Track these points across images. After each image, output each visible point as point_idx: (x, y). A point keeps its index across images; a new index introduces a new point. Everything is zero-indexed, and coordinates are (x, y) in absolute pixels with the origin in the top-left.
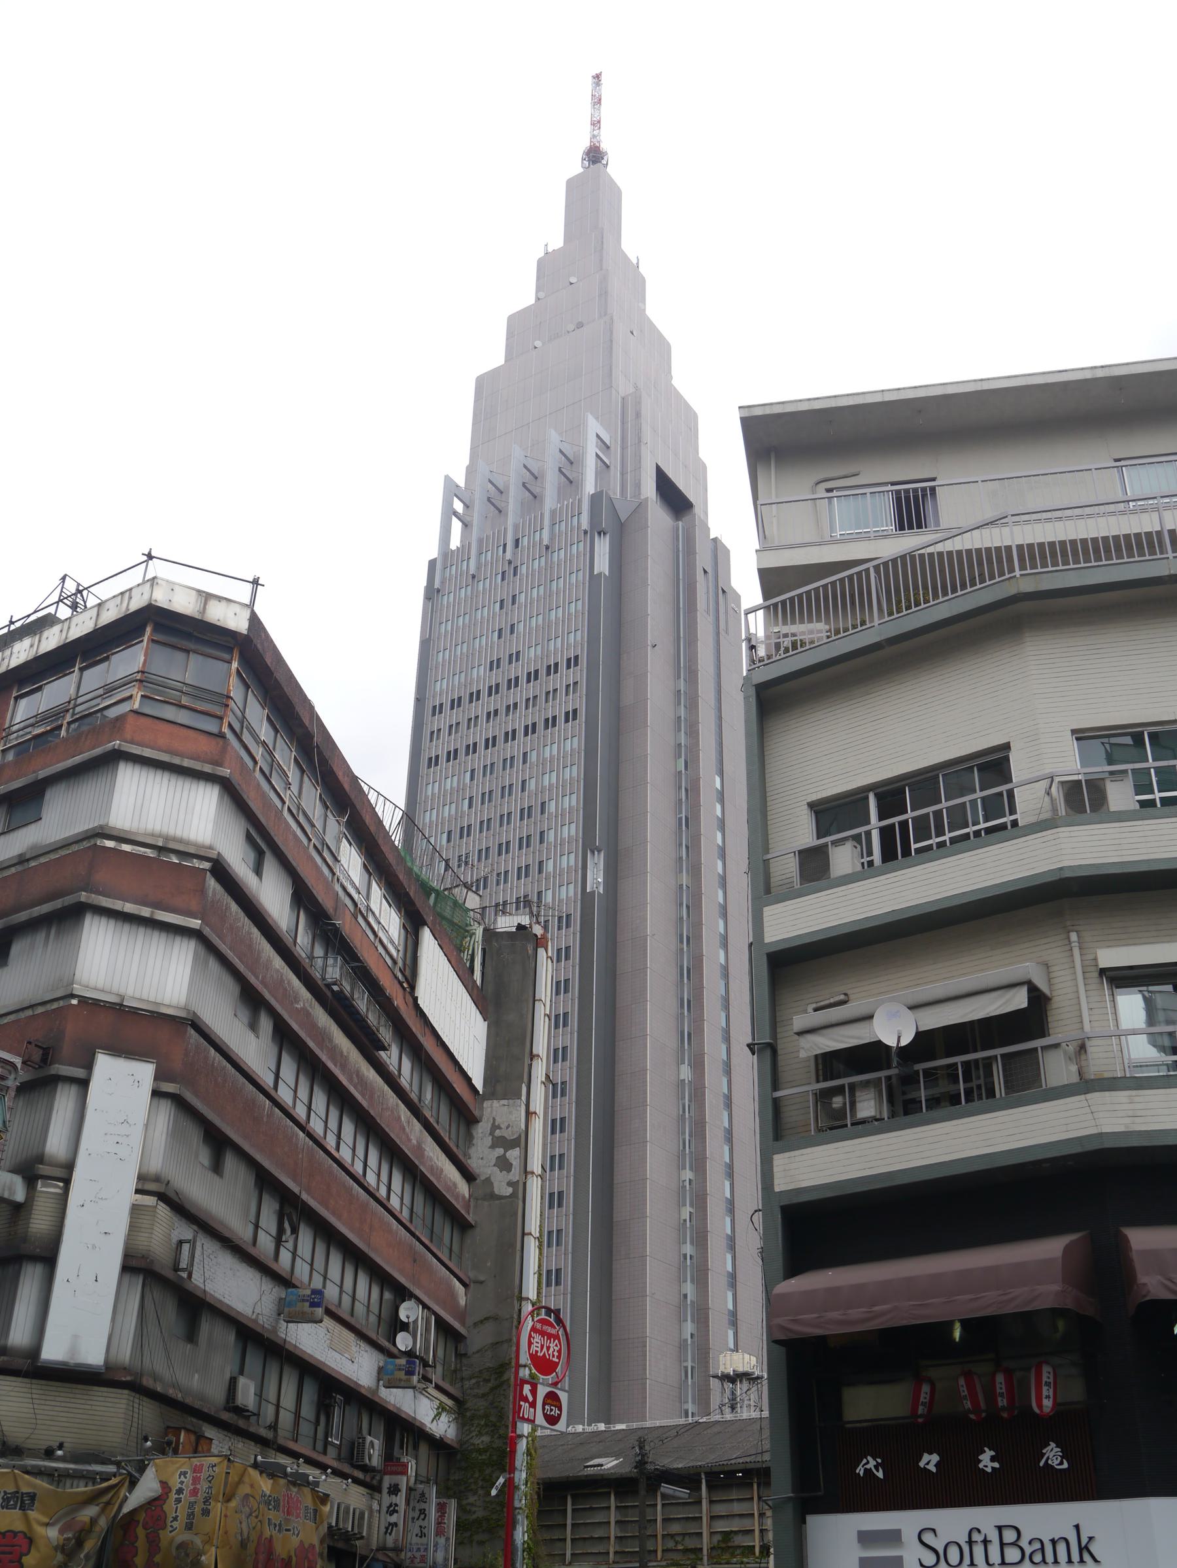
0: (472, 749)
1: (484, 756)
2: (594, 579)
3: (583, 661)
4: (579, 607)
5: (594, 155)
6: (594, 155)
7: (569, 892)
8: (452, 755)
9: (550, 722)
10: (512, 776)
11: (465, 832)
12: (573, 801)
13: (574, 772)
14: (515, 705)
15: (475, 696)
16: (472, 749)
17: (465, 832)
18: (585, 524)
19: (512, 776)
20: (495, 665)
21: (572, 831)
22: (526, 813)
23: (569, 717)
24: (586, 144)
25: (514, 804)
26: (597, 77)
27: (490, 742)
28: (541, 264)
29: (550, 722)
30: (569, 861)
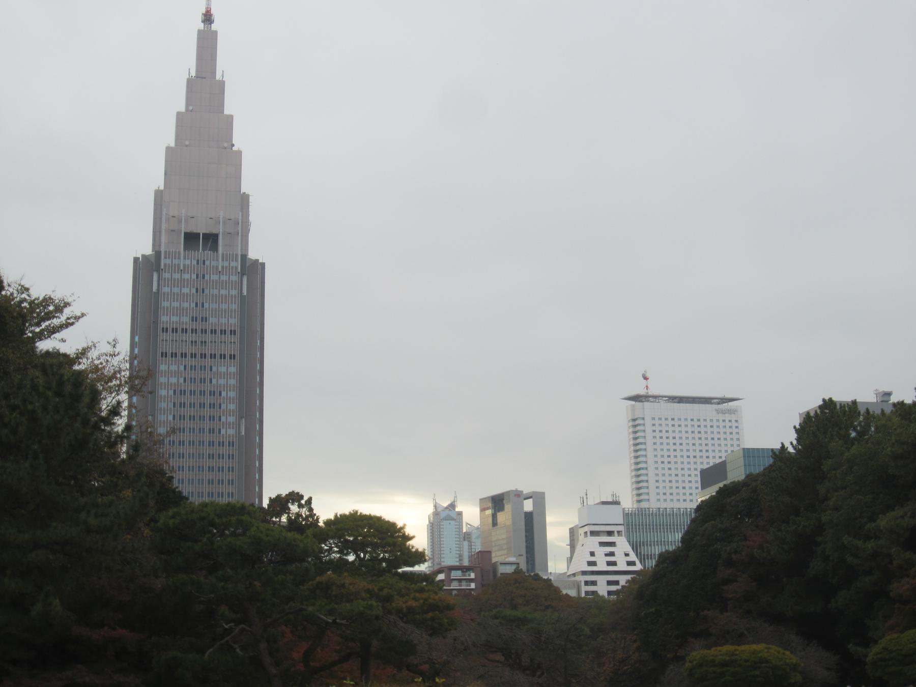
0: (184, 355)
1: (190, 362)
2: (242, 297)
3: (238, 333)
5: (208, 18)
6: (208, 18)
8: (174, 355)
9: (223, 356)
12: (232, 394)
13: (232, 382)
14: (205, 342)
15: (185, 331)
16: (184, 355)
18: (239, 270)
20: (195, 319)
21: (232, 407)
22: (212, 393)
23: (233, 357)
24: (204, 11)
27: (193, 356)
29: (223, 356)
30: (231, 419)
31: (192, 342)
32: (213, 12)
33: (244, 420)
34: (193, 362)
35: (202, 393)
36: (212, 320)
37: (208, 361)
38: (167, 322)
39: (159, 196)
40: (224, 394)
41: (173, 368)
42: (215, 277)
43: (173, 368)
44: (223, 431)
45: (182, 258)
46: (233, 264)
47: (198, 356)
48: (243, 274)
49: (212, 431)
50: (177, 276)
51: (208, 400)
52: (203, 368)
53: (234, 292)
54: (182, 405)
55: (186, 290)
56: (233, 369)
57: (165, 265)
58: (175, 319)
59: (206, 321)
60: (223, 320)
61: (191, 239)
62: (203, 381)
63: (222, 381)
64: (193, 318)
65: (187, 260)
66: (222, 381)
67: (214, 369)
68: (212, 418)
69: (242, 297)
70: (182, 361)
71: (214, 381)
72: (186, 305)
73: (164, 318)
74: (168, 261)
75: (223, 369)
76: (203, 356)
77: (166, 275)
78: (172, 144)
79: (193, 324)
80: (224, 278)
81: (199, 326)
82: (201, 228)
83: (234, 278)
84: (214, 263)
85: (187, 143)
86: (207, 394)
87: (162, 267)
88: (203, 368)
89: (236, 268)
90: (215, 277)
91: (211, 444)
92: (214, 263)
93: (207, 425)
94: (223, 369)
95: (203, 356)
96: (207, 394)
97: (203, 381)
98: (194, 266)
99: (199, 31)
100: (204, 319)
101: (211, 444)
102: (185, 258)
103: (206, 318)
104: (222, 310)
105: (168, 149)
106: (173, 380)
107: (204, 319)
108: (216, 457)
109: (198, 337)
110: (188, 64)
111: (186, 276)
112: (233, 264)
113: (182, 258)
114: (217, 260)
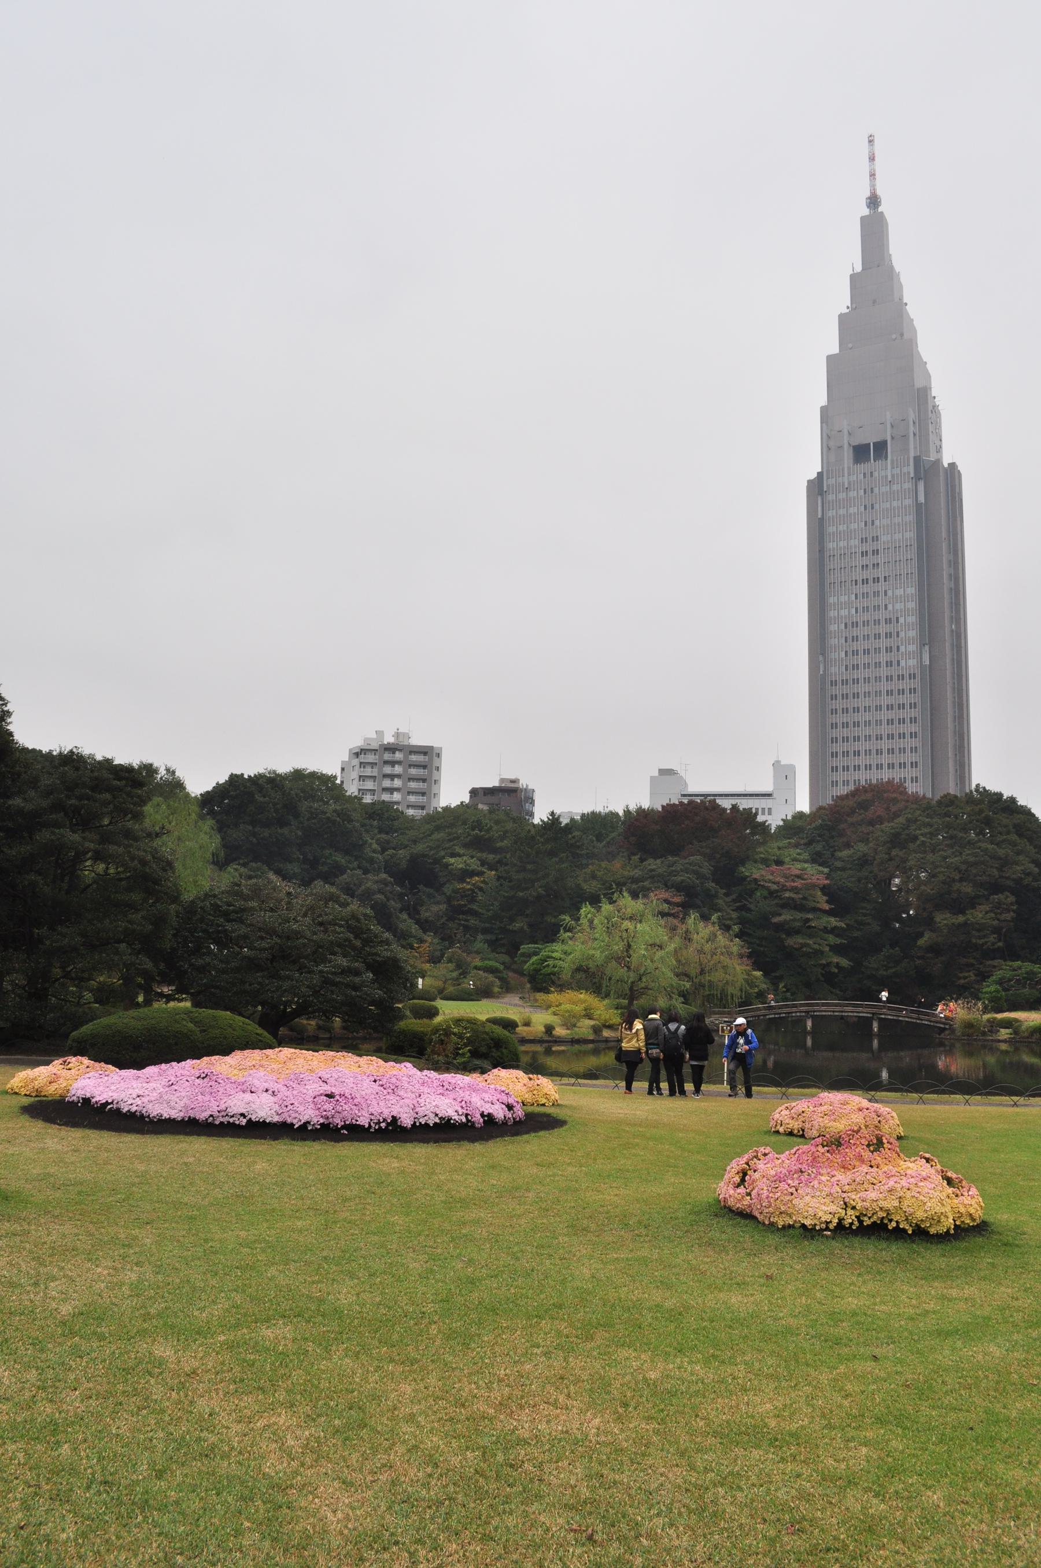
4: (910, 518)
5: (874, 201)
6: (874, 201)
7: (912, 662)
10: (881, 601)
11: (855, 624)
12: (912, 619)
13: (912, 605)
14: (878, 564)
17: (855, 624)
18: (912, 475)
19: (881, 601)
21: (912, 633)
22: (888, 621)
24: (868, 194)
25: (882, 615)
26: (871, 142)
27: (865, 581)
28: (851, 276)
30: (912, 648)
31: (863, 566)
32: (879, 192)
33: (927, 648)
34: (866, 589)
35: (877, 622)
36: (884, 538)
37: (881, 586)
38: (834, 549)
39: (824, 411)
40: (902, 620)
41: (843, 599)
42: (884, 489)
43: (843, 599)
44: (903, 663)
45: (846, 474)
46: (905, 470)
47: (871, 581)
48: (917, 478)
49: (889, 664)
50: (842, 496)
51: (883, 629)
52: (876, 594)
53: (908, 502)
54: (855, 639)
55: (852, 510)
56: (911, 591)
57: (828, 486)
58: (842, 544)
59: (877, 540)
60: (897, 536)
61: (861, 453)
62: (877, 608)
63: (898, 606)
64: (862, 539)
65: (853, 474)
66: (898, 606)
67: (890, 593)
68: (889, 650)
69: (918, 506)
70: (852, 590)
71: (890, 607)
72: (854, 526)
73: (831, 545)
74: (832, 481)
75: (899, 592)
76: (876, 580)
77: (831, 497)
78: (835, 349)
79: (862, 546)
80: (895, 487)
81: (869, 547)
82: (870, 438)
83: (907, 485)
84: (883, 473)
85: (850, 345)
86: (883, 622)
87: (825, 489)
88: (876, 594)
89: (909, 473)
90: (885, 489)
91: (889, 678)
92: (883, 473)
93: (883, 658)
94: (899, 592)
95: (876, 580)
96: (883, 622)
97: (877, 608)
98: (861, 480)
99: (863, 219)
100: (875, 539)
101: (889, 678)
102: (849, 475)
103: (877, 537)
104: (895, 524)
105: (830, 358)
106: (844, 612)
107: (875, 539)
108: (895, 693)
109: (869, 560)
110: (853, 259)
111: (853, 494)
112: (905, 470)
113: (846, 474)
114: (886, 469)
